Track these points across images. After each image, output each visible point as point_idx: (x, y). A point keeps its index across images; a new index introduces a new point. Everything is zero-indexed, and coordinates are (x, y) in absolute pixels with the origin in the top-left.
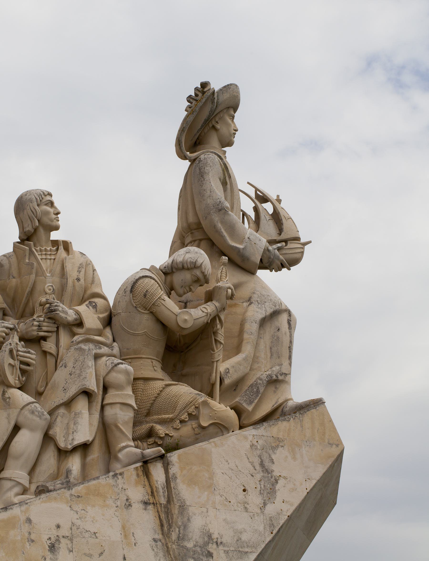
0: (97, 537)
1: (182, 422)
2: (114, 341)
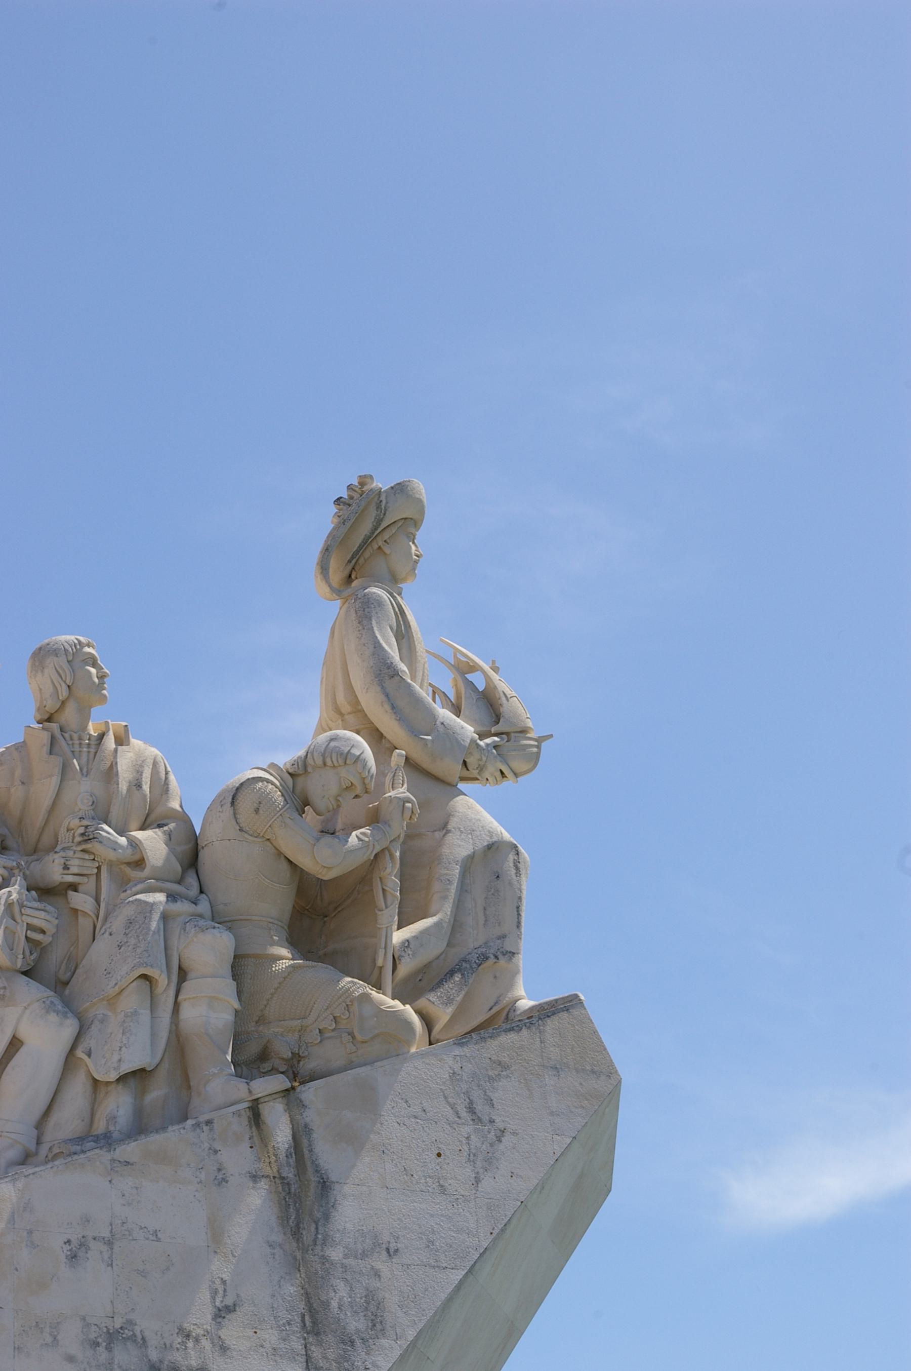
2: (201, 892)
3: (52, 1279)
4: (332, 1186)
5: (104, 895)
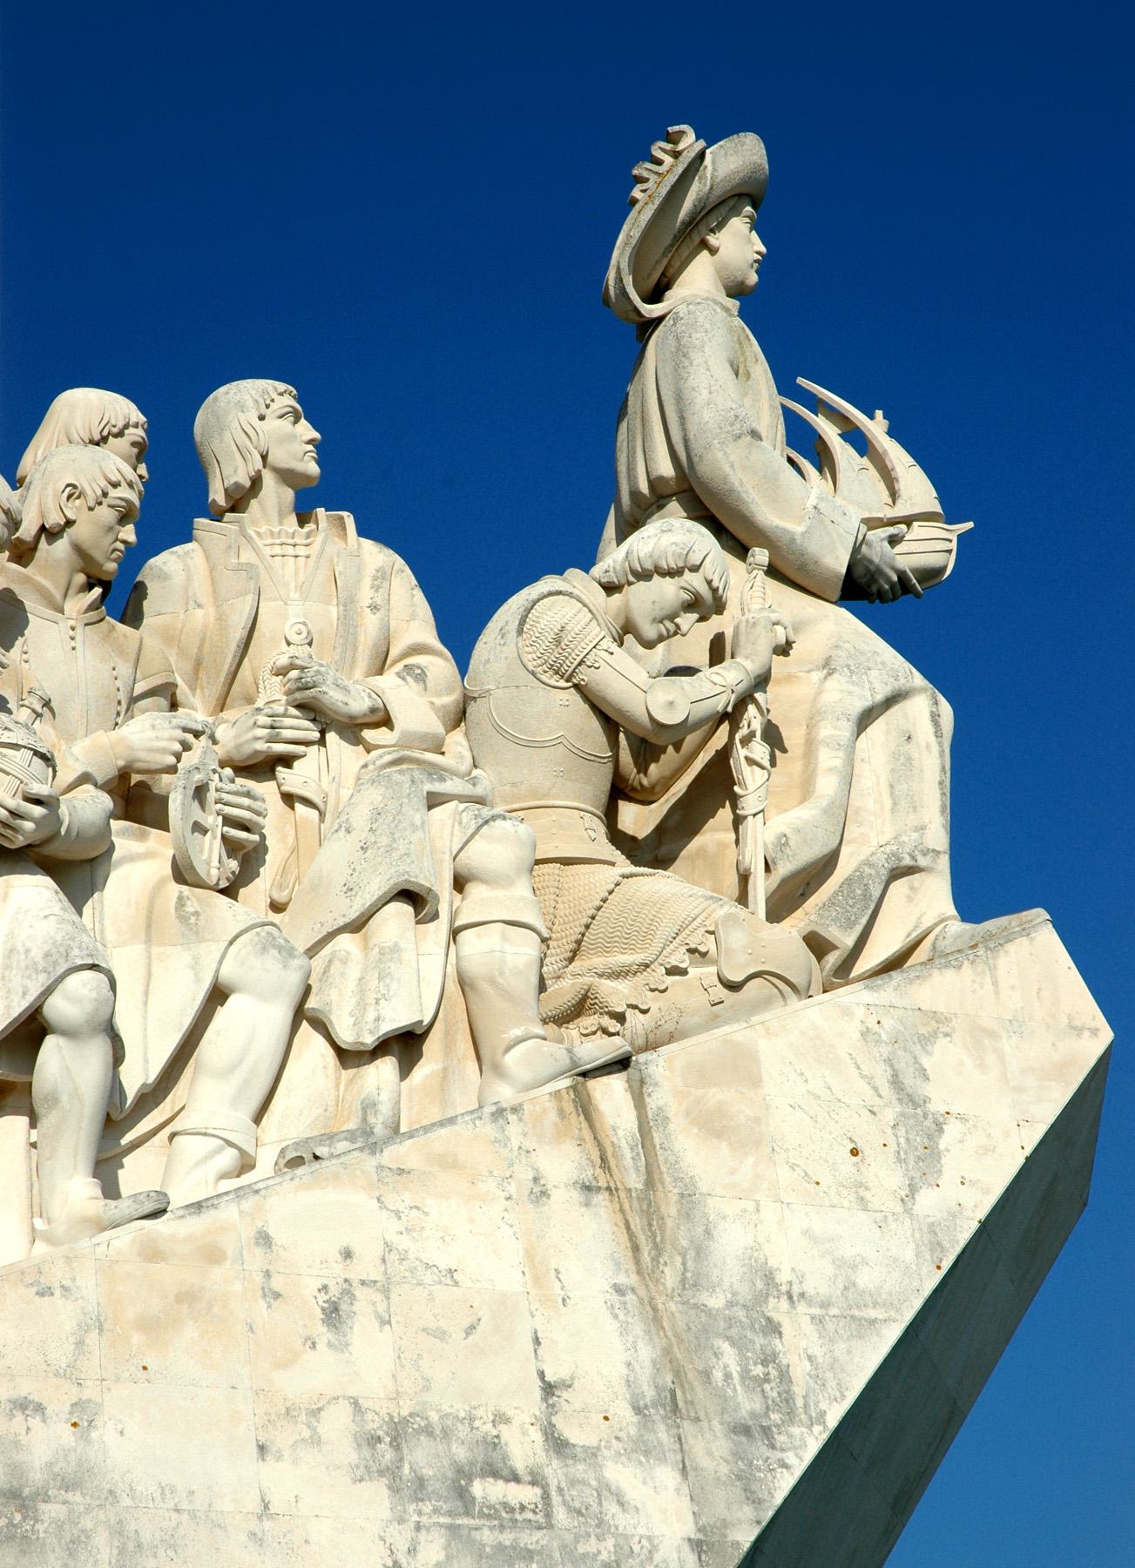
0: (457, 1283)
1: (673, 971)
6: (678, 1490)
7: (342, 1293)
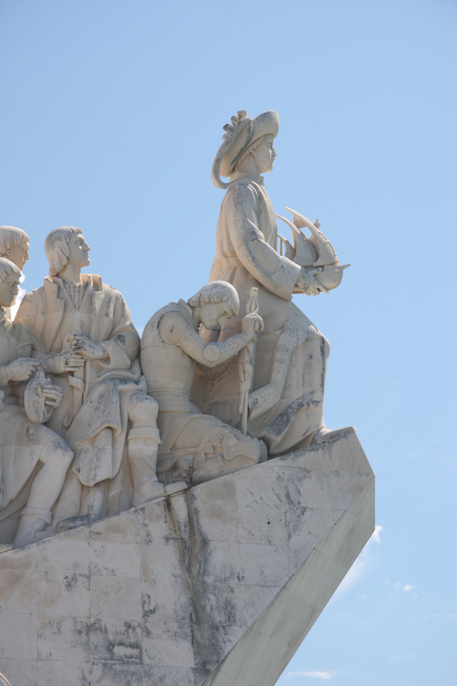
2: (142, 374)
3: (58, 598)
4: (209, 542)
5: (88, 379)
6: (189, 650)
7: (73, 579)
